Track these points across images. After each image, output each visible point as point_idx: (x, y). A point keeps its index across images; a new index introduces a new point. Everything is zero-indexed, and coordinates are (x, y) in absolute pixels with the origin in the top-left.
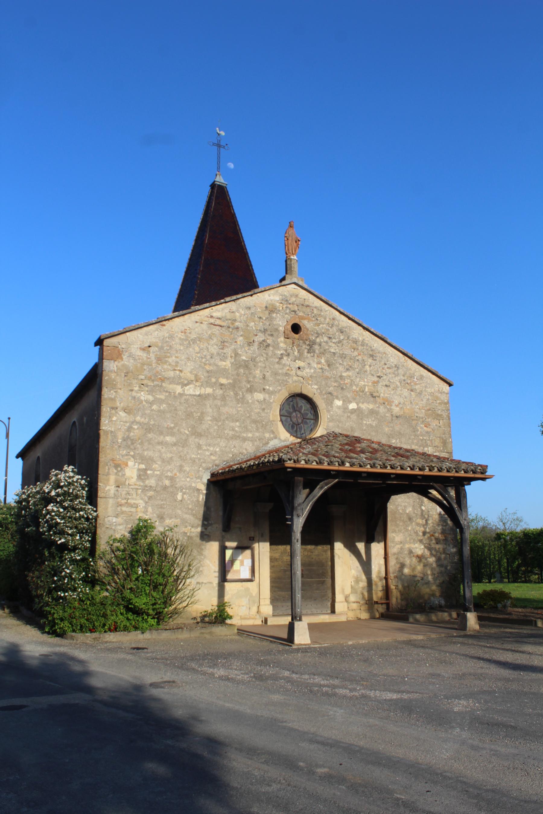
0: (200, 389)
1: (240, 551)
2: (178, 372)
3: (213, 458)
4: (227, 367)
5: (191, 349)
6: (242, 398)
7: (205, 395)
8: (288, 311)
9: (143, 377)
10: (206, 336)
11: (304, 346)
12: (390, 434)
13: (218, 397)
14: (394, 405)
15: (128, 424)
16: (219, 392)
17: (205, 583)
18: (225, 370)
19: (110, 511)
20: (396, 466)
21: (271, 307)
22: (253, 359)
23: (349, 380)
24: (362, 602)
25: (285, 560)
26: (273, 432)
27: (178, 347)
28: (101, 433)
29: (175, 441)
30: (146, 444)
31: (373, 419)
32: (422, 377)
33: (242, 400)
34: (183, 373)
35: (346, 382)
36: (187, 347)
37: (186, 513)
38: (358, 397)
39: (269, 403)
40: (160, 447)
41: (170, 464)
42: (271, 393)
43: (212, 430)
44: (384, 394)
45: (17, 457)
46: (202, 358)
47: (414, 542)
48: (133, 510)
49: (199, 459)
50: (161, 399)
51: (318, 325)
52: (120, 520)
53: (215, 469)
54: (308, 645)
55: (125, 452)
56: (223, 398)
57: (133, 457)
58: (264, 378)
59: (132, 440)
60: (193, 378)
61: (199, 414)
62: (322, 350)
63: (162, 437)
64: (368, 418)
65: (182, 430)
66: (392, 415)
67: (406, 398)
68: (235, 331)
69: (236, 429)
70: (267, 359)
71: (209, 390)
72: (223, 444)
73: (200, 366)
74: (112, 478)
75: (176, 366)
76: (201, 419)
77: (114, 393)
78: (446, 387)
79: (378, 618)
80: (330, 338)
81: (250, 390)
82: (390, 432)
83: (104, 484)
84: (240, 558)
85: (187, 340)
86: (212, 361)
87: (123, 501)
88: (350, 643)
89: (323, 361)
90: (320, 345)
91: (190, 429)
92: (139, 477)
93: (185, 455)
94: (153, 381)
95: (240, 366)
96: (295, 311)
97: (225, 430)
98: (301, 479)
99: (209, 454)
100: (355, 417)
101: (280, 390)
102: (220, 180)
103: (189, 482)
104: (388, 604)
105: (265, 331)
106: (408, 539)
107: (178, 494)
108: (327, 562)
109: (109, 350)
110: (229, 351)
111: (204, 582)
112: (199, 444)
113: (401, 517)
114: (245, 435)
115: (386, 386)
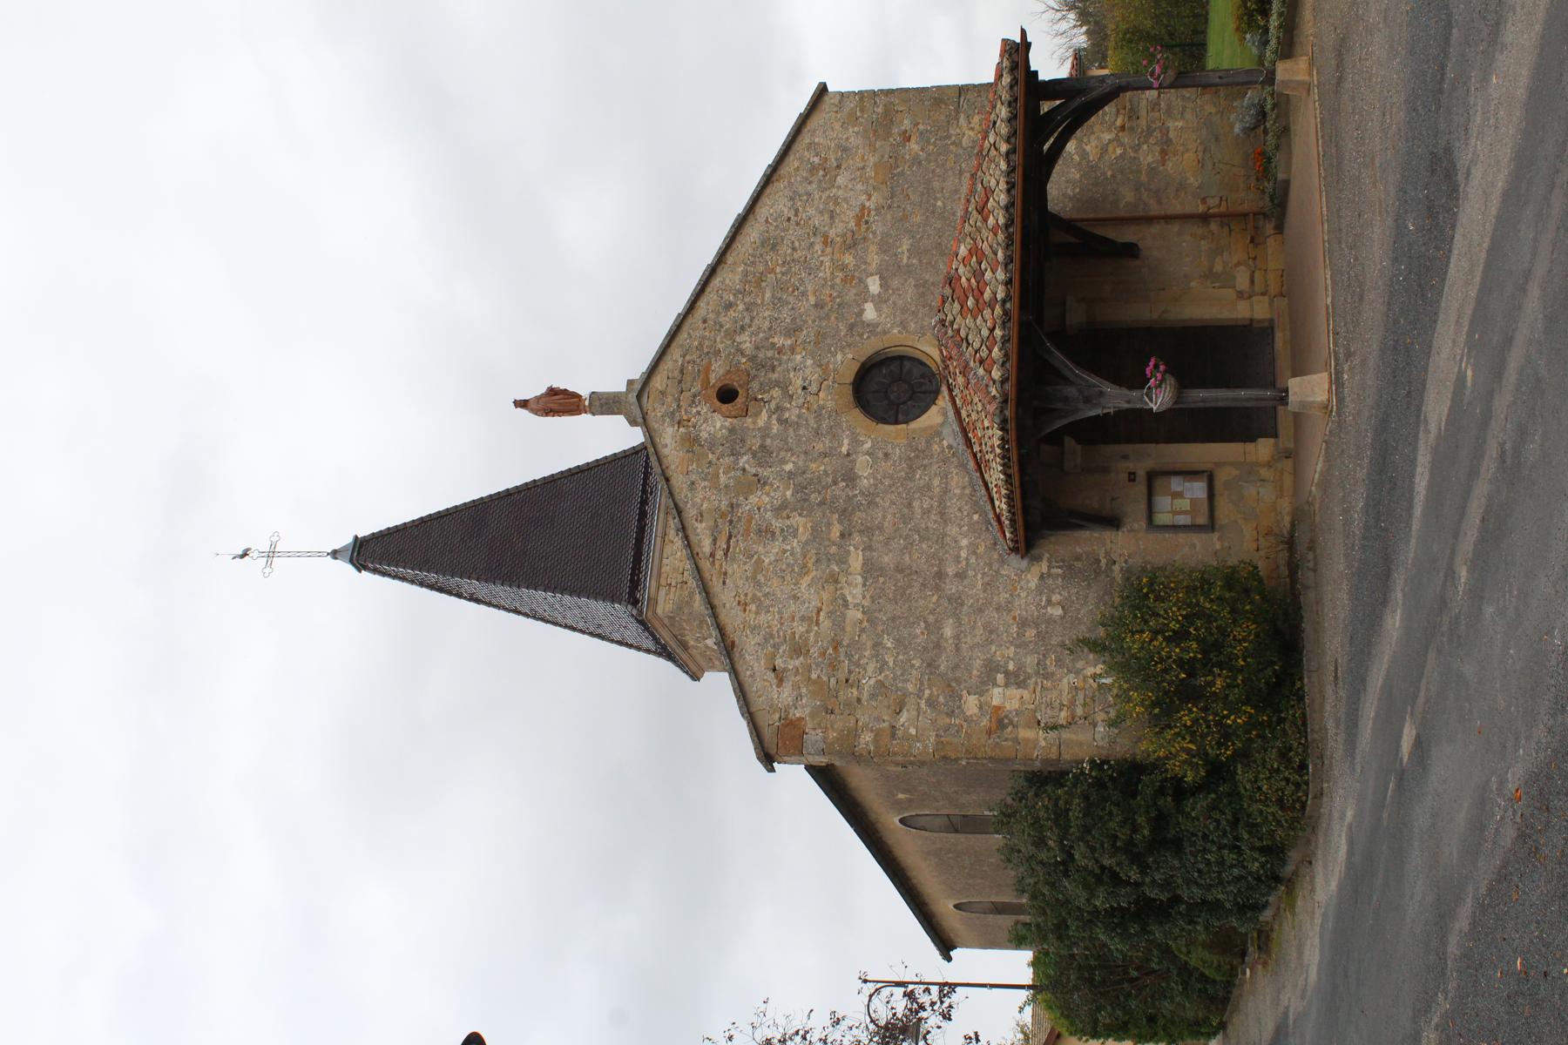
3: (981, 550)
39: (870, 447)
42: (855, 442)
45: (949, 959)
48: (1081, 695)
53: (1003, 546)
56: (867, 531)
61: (899, 576)
71: (856, 561)
74: (1024, 733)
80: (742, 328)
81: (851, 478)
92: (1021, 685)
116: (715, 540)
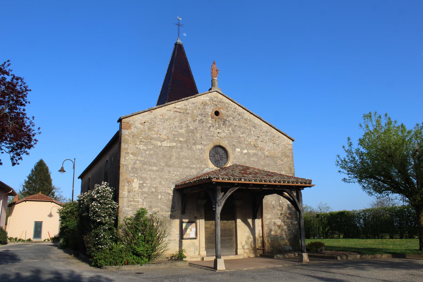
3: (176, 177)
9: (141, 138)
10: (173, 117)
16: (179, 145)
18: (182, 134)
19: (125, 204)
22: (196, 129)
24: (251, 249)
26: (206, 165)
28: (121, 165)
32: (279, 137)
33: (190, 149)
40: (150, 172)
42: (205, 145)
43: (175, 164)
45: (79, 178)
47: (276, 219)
48: (137, 204)
49: (170, 178)
52: (130, 209)
53: (178, 183)
56: (181, 148)
57: (137, 177)
60: (166, 138)
62: (230, 124)
63: (151, 167)
65: (161, 164)
68: (187, 115)
71: (174, 144)
72: (181, 170)
73: (170, 132)
74: (126, 188)
75: (158, 132)
76: (170, 158)
78: (291, 142)
79: (259, 257)
80: (234, 118)
81: (195, 144)
84: (190, 227)
86: (176, 130)
88: (245, 269)
89: (230, 129)
90: (229, 121)
92: (140, 187)
94: (146, 139)
102: (179, 41)
104: (264, 250)
105: (202, 114)
110: (184, 125)
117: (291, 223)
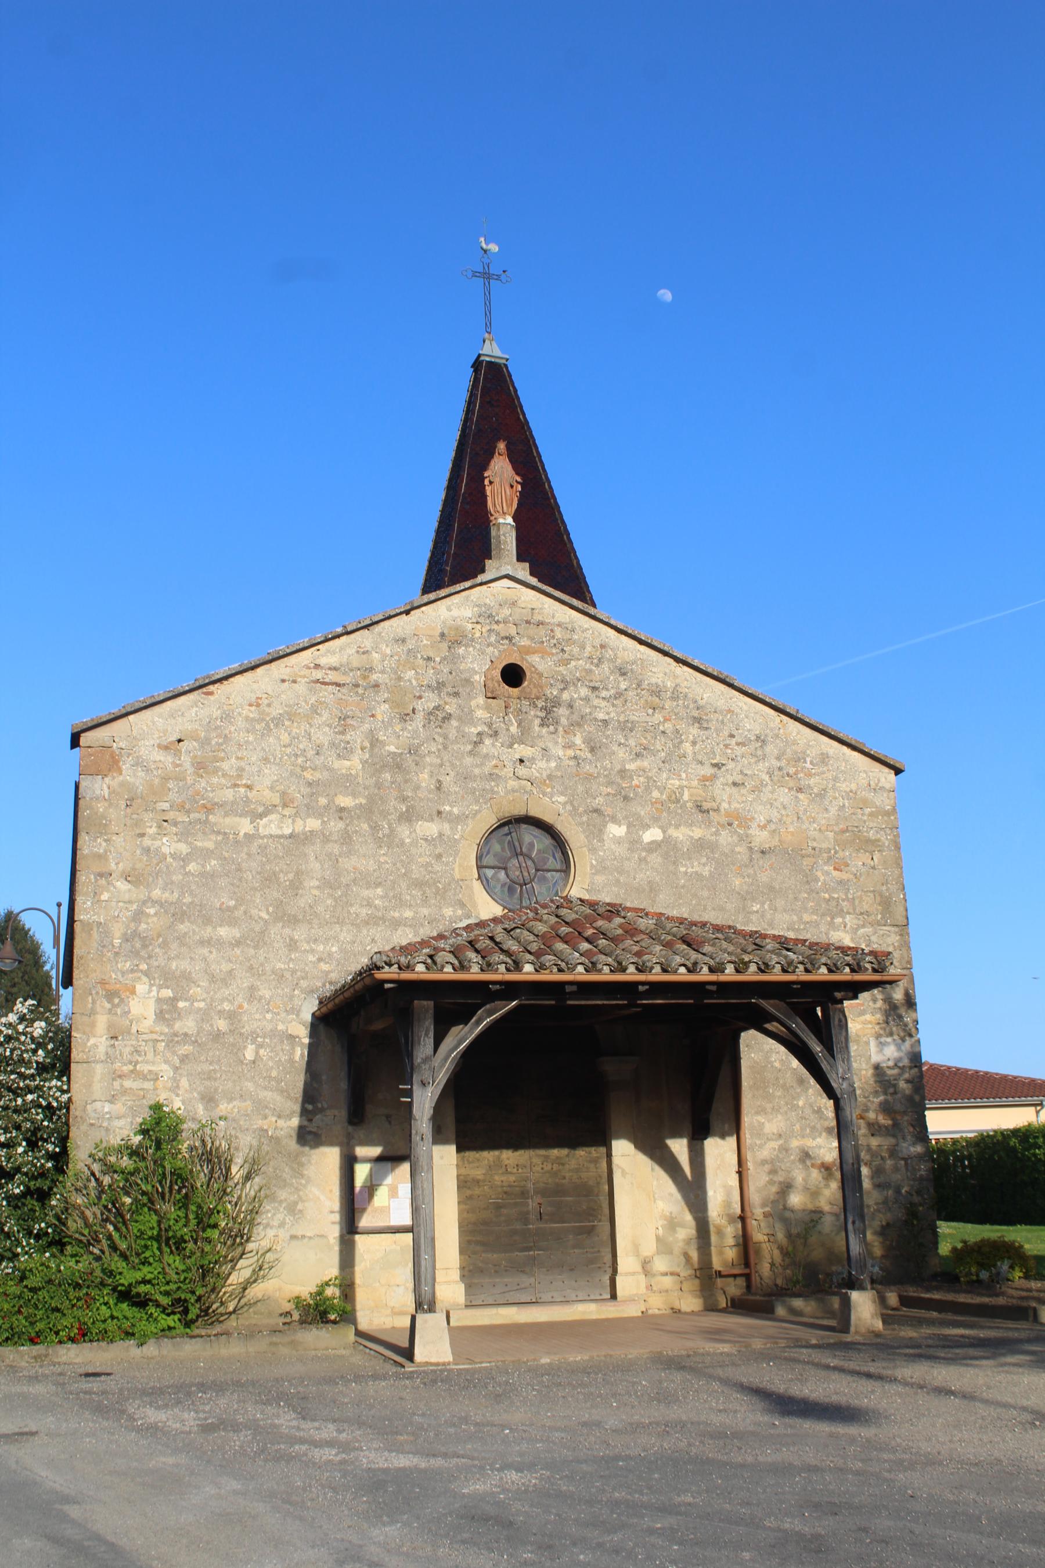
0: (294, 821)
1: (389, 1165)
2: (242, 790)
3: (324, 967)
4: (353, 772)
5: (271, 740)
6: (388, 836)
7: (304, 833)
8: (493, 639)
9: (166, 806)
11: (532, 713)
12: (748, 893)
13: (335, 837)
14: (754, 825)
15: (135, 907)
16: (336, 826)
17: (310, 1238)
18: (349, 777)
19: (98, 1088)
20: (649, 964)
21: (453, 633)
22: (413, 750)
23: (642, 779)
24: (686, 1272)
25: (499, 1183)
26: (462, 905)
27: (242, 737)
29: (238, 935)
30: (174, 946)
31: (704, 860)
32: (824, 758)
33: (390, 840)
34: (254, 792)
35: (635, 782)
36: (263, 735)
37: (265, 1088)
38: (665, 814)
40: (205, 951)
41: (227, 985)
43: (320, 909)
44: (729, 803)
46: (296, 756)
49: (293, 972)
50: (208, 849)
51: (567, 662)
52: (119, 1108)
54: (449, 1363)
55: (128, 964)
56: (346, 838)
57: (146, 974)
58: (439, 789)
59: (143, 939)
60: (277, 800)
62: (575, 717)
63: (209, 929)
64: (690, 859)
65: (254, 912)
66: (750, 849)
67: (785, 808)
69: (377, 902)
70: (445, 748)
71: (313, 824)
72: (345, 936)
73: (292, 774)
74: (102, 1021)
75: (240, 777)
76: (296, 886)
77: (104, 844)
78: (887, 777)
79: (723, 1311)
80: (594, 689)
81: (408, 817)
82: (745, 887)
83: (84, 1033)
84: (389, 1180)
85: (263, 720)
86: (319, 761)
87: (125, 1068)
88: (545, 1360)
90: (571, 706)
91: (271, 909)
92: (160, 1016)
93: (262, 965)
94: (188, 812)
95: (384, 766)
96: (510, 638)
97: (351, 905)
98: (431, 1003)
99: (314, 959)
100: (659, 860)
101: (477, 812)
102: (492, 351)
103: (271, 1021)
104: (748, 1277)
105: (440, 686)
106: (797, 1127)
107: (245, 1047)
108: (598, 1183)
109: (91, 755)
110: (356, 737)
111: (308, 1234)
112: (291, 939)
113: (777, 1079)
114: (397, 915)
115: (735, 784)
116: (335, 669)
117: (893, 1152)
